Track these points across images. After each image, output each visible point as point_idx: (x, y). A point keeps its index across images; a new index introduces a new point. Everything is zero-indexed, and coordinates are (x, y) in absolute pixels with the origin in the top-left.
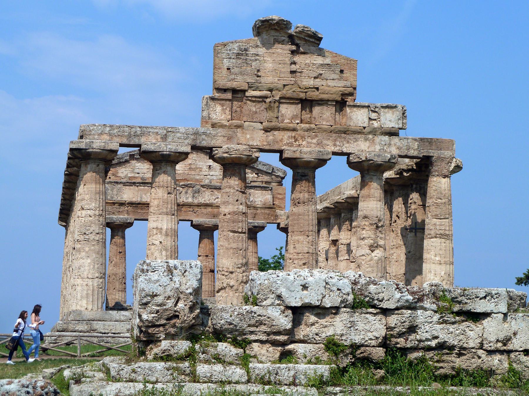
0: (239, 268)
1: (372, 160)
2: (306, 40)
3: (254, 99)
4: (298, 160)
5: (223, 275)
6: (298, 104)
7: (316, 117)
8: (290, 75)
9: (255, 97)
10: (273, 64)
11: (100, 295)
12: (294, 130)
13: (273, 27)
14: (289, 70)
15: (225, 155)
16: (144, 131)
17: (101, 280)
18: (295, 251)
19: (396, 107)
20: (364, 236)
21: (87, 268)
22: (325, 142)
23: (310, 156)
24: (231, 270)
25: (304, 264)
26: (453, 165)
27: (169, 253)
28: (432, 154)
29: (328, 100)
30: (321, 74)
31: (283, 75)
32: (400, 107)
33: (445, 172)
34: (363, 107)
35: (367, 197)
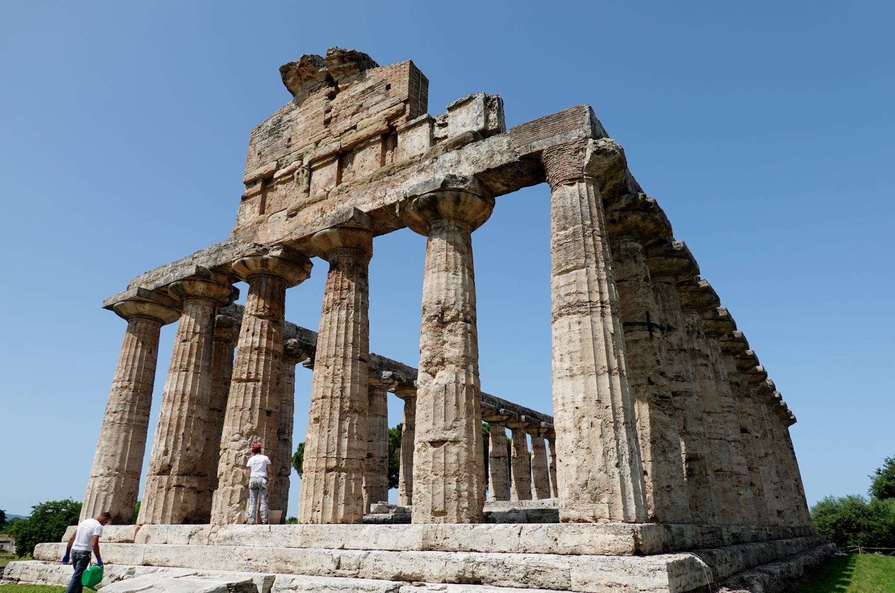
0: (235, 440)
1: (415, 196)
2: (343, 70)
3: (283, 179)
6: (333, 161)
7: (356, 170)
8: (323, 127)
10: (306, 122)
11: (102, 501)
13: (304, 76)
14: (322, 121)
17: (108, 479)
19: (471, 99)
22: (359, 200)
25: (317, 420)
26: (589, 153)
27: (166, 429)
28: (538, 148)
29: (370, 137)
30: (361, 106)
32: (480, 98)
33: (570, 171)
34: (421, 123)
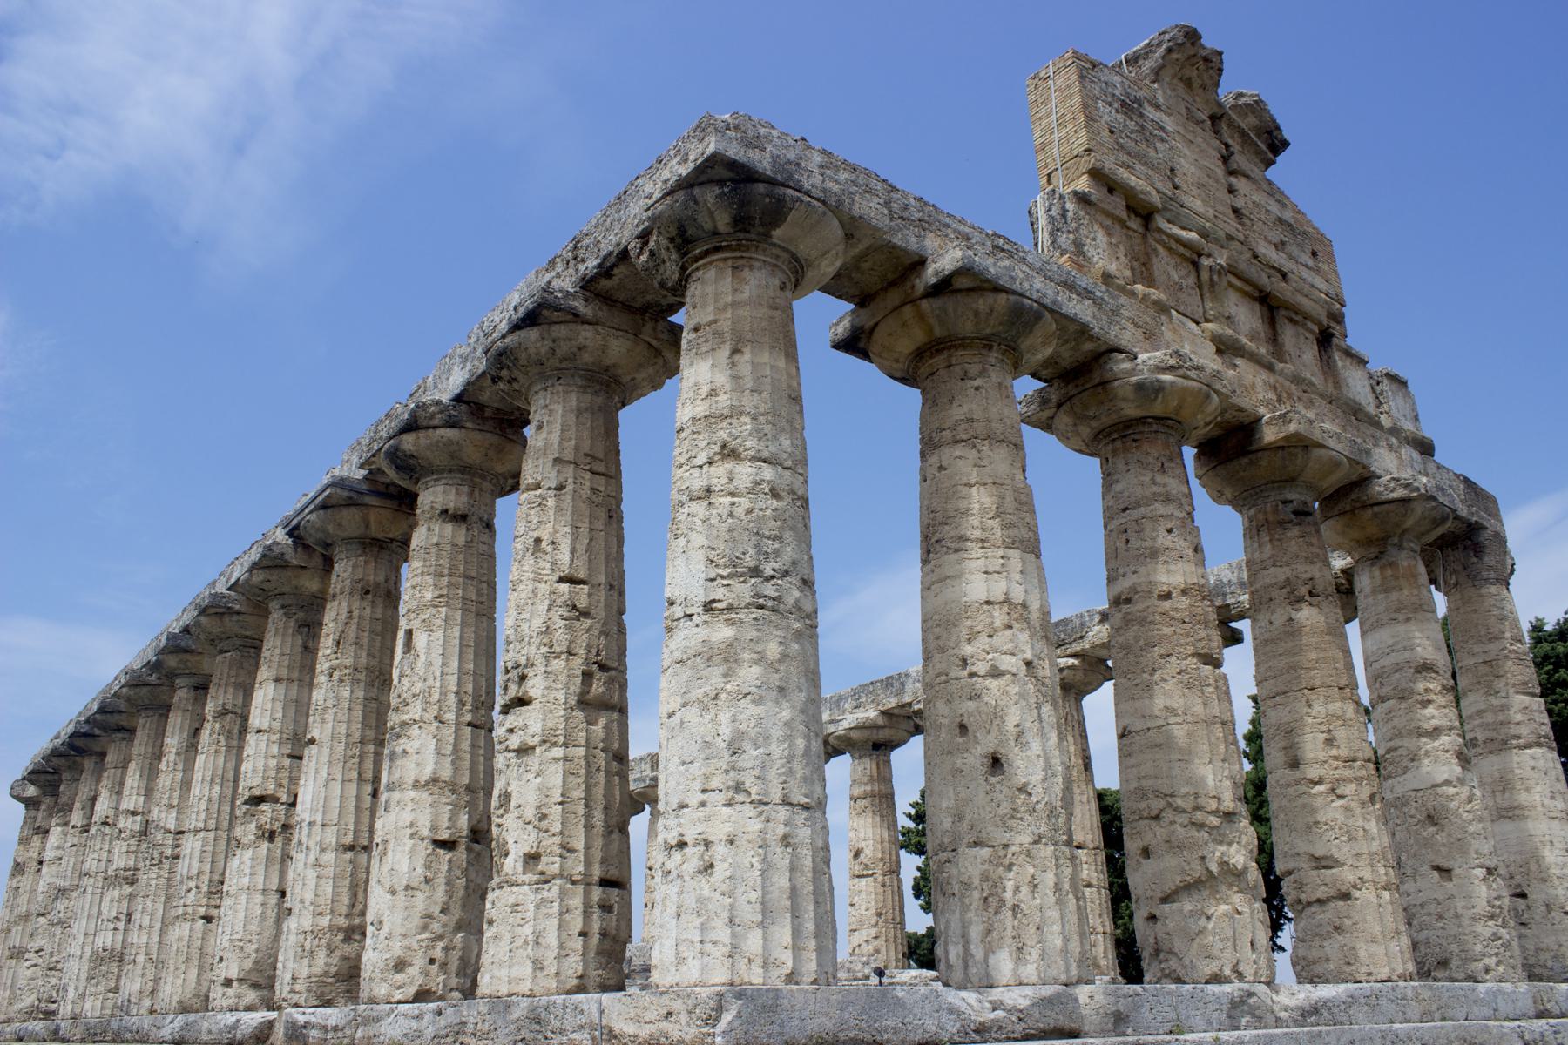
3: (1174, 245)
4: (1317, 452)
5: (1201, 826)
6: (1255, 299)
9: (1178, 240)
12: (1270, 368)
15: (1167, 377)
16: (930, 219)
18: (1334, 752)
20: (1434, 722)
21: (778, 750)
23: (1339, 447)
24: (1229, 803)
31: (1220, 208)
35: (1415, 611)
